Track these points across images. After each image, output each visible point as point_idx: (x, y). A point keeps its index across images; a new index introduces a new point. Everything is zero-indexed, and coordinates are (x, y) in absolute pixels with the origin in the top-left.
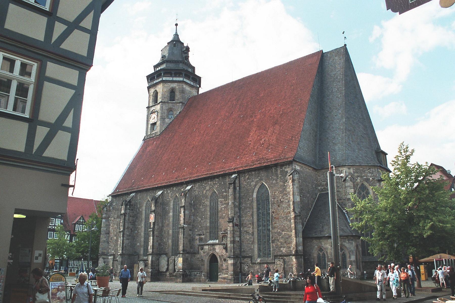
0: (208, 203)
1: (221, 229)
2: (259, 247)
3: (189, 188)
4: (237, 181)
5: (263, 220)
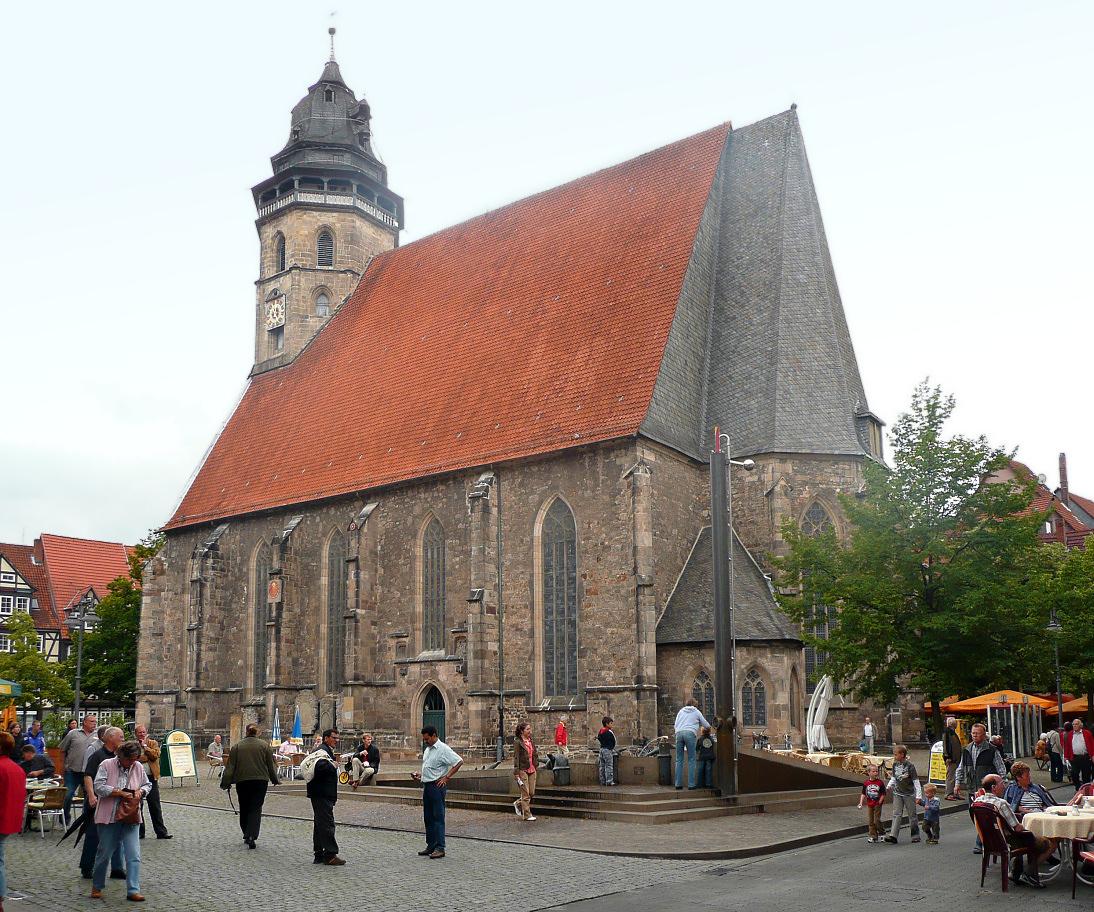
0: (419, 551)
1: (452, 620)
2: (547, 668)
3: (368, 508)
4: (493, 492)
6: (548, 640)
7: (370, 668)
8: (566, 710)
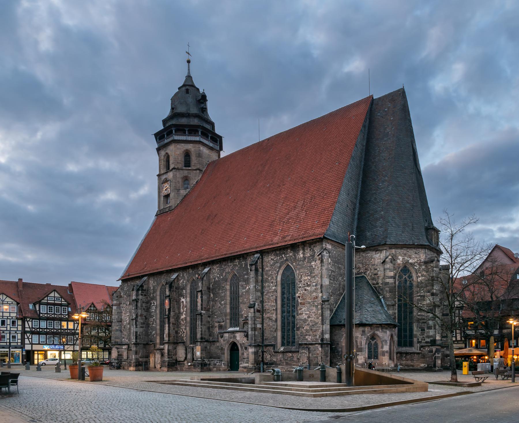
0: (228, 287)
1: (242, 315)
3: (206, 270)
5: (287, 305)
6: (283, 323)
8: (290, 352)
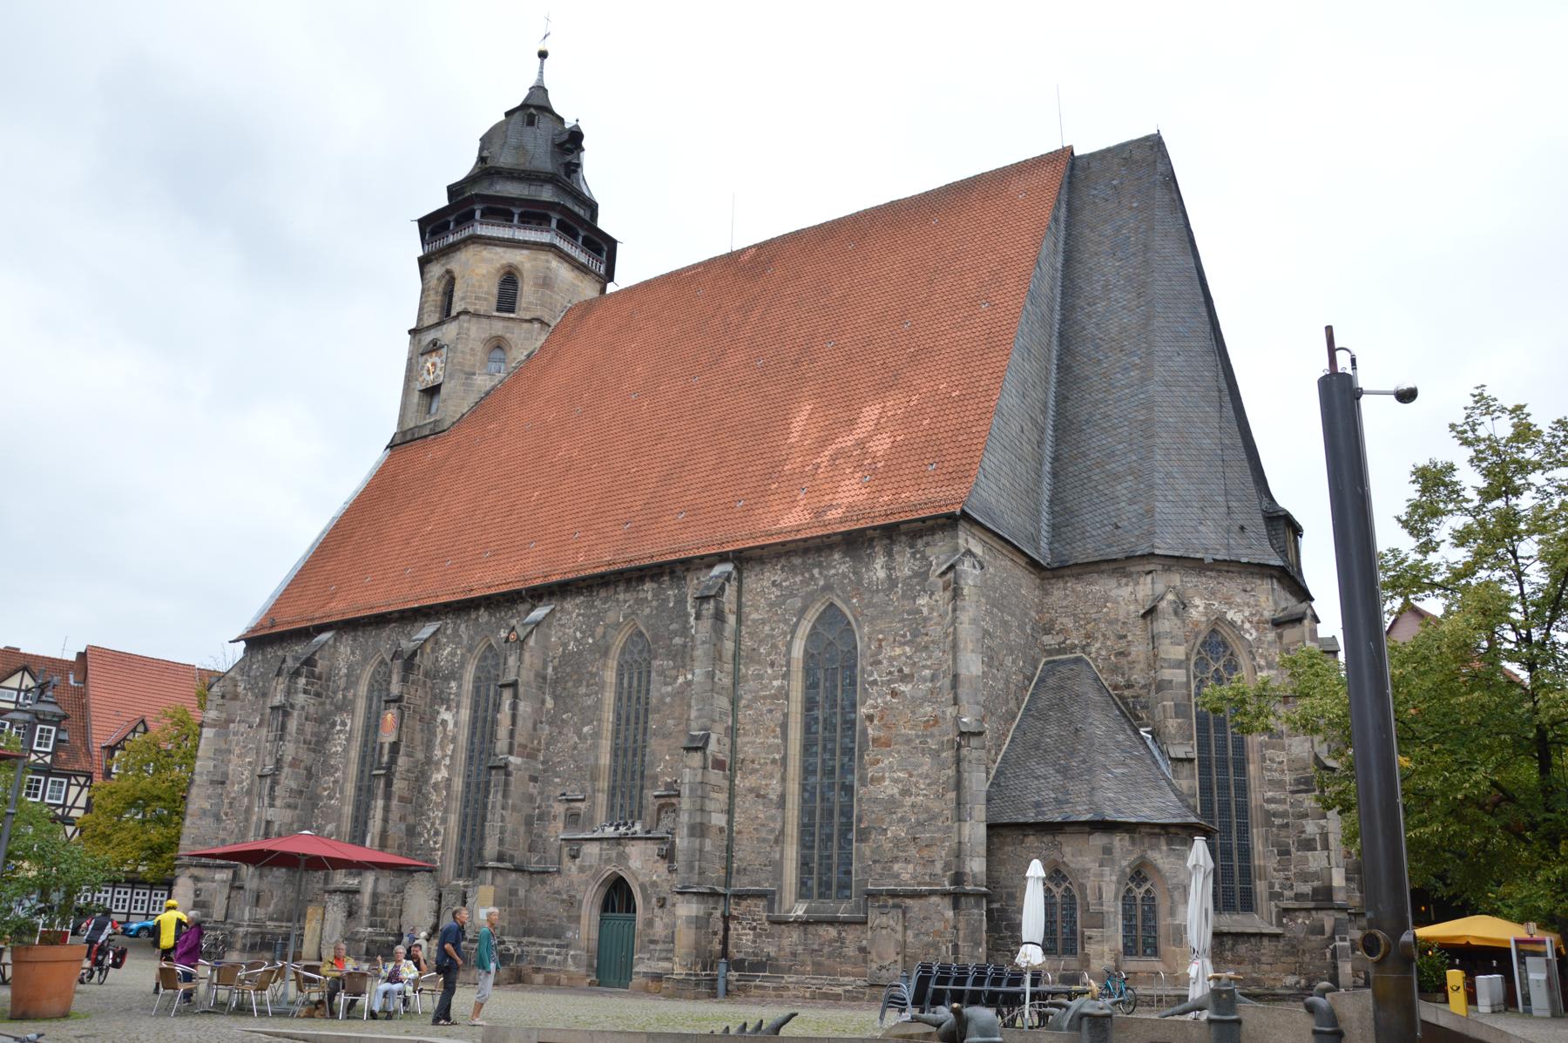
0: (610, 676)
1: (655, 778)
2: (803, 857)
3: (539, 613)
4: (730, 591)
7: (523, 843)
